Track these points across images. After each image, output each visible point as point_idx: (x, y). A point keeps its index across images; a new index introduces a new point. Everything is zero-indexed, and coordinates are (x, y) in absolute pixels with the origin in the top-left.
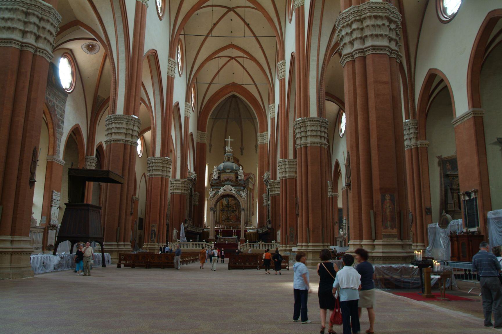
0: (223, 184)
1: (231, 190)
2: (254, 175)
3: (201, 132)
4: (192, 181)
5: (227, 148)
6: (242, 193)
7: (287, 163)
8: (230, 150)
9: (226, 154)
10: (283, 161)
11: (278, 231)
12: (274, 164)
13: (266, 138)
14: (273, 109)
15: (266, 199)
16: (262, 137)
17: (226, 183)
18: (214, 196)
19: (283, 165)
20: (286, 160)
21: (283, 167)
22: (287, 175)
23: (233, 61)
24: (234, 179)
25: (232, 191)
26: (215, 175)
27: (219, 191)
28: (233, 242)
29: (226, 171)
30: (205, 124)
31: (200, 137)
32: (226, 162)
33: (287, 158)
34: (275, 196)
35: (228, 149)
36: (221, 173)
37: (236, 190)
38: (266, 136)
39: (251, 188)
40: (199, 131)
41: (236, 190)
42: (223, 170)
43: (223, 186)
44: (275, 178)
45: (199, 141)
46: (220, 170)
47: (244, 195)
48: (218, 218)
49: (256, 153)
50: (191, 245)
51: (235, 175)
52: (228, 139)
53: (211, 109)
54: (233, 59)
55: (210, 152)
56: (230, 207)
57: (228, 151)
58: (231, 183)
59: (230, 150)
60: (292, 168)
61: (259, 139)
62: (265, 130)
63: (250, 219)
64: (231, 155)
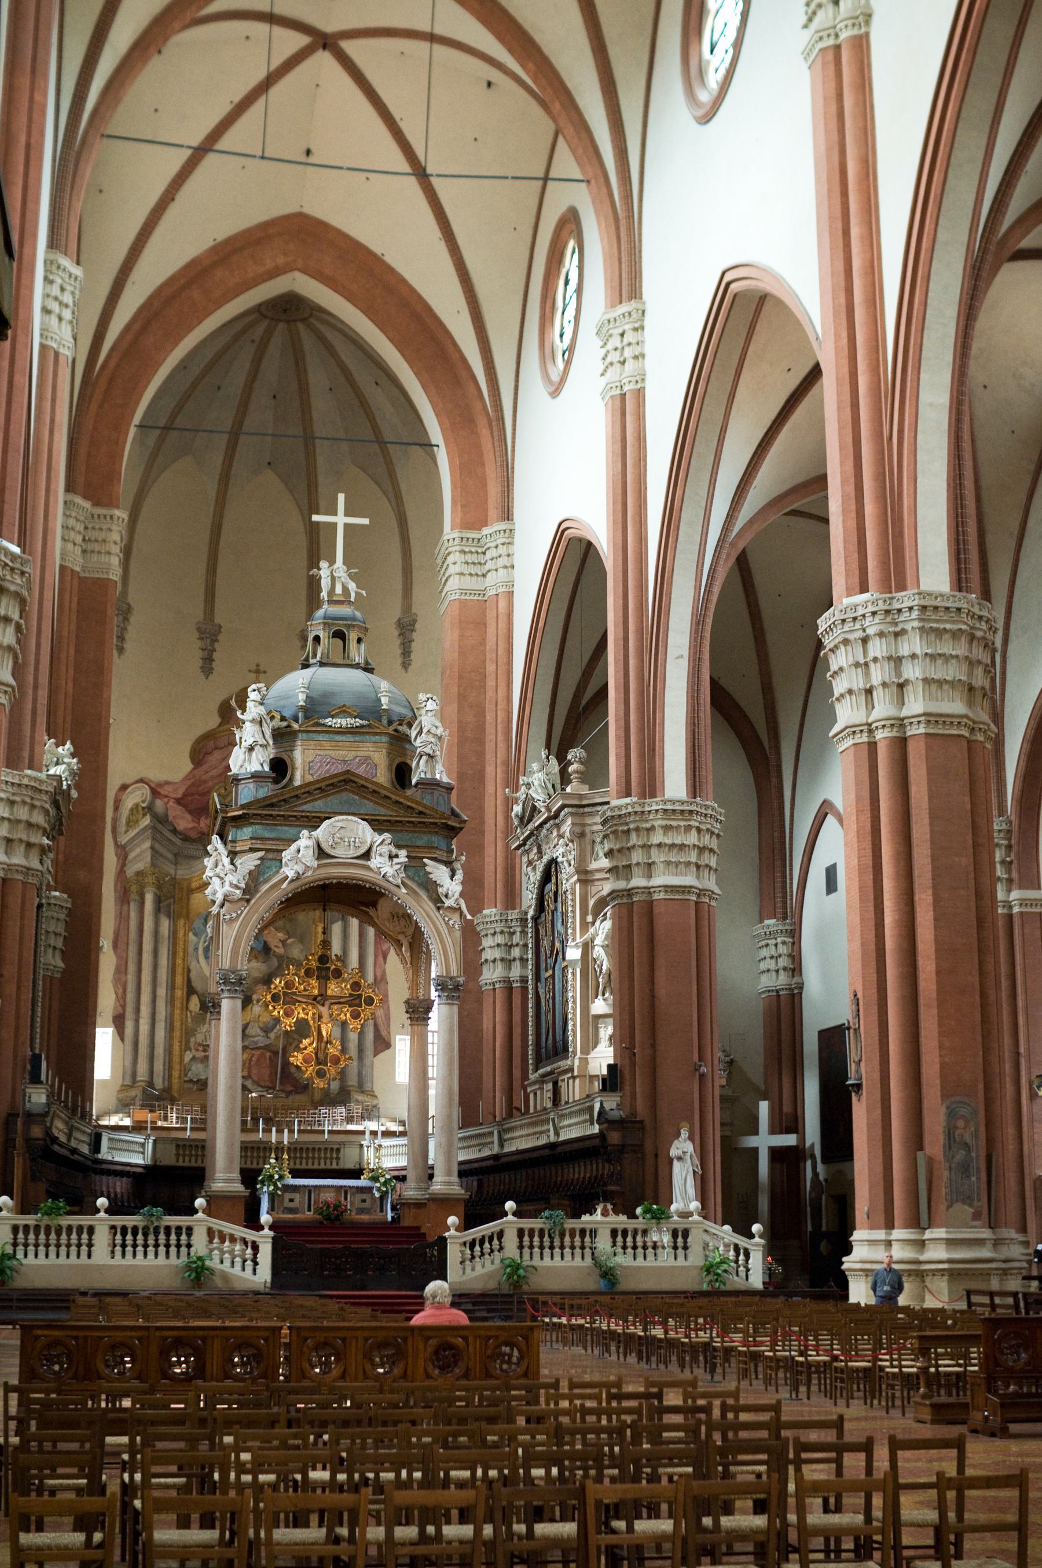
0: (319, 805)
1: (367, 855)
3: (87, 505)
4: (58, 797)
5: (324, 571)
6: (439, 873)
7: (911, 621)
8: (345, 589)
9: (320, 613)
10: (882, 606)
11: (679, 1135)
12: (641, 693)
13: (501, 562)
14: (629, 337)
15: (500, 939)
16: (469, 558)
17: (333, 801)
18: (250, 890)
19: (881, 634)
20: (906, 599)
21: (877, 648)
22: (915, 705)
23: (324, 60)
24: (383, 776)
25: (375, 862)
26: (251, 749)
27: (286, 855)
28: (365, 1217)
29: (329, 721)
30: (116, 456)
31: (79, 539)
32: (322, 664)
33: (902, 587)
34: (650, 904)
35: (333, 579)
36: (295, 733)
37: (403, 853)
38: (502, 550)
40: (78, 500)
41: (403, 853)
42: (306, 717)
43: (314, 822)
44: (651, 786)
45: (76, 564)
46: (287, 714)
47: (451, 886)
48: (159, 1066)
49: (406, 665)
50: (102, 1238)
51: (389, 754)
52: (335, 513)
53: (159, 364)
54: (325, 47)
55: (121, 650)
56: (338, 974)
57: (332, 591)
58: (369, 807)
59: (345, 589)
60: (946, 658)
61: (452, 569)
62: (493, 512)
63: (360, 1074)
64: (354, 619)
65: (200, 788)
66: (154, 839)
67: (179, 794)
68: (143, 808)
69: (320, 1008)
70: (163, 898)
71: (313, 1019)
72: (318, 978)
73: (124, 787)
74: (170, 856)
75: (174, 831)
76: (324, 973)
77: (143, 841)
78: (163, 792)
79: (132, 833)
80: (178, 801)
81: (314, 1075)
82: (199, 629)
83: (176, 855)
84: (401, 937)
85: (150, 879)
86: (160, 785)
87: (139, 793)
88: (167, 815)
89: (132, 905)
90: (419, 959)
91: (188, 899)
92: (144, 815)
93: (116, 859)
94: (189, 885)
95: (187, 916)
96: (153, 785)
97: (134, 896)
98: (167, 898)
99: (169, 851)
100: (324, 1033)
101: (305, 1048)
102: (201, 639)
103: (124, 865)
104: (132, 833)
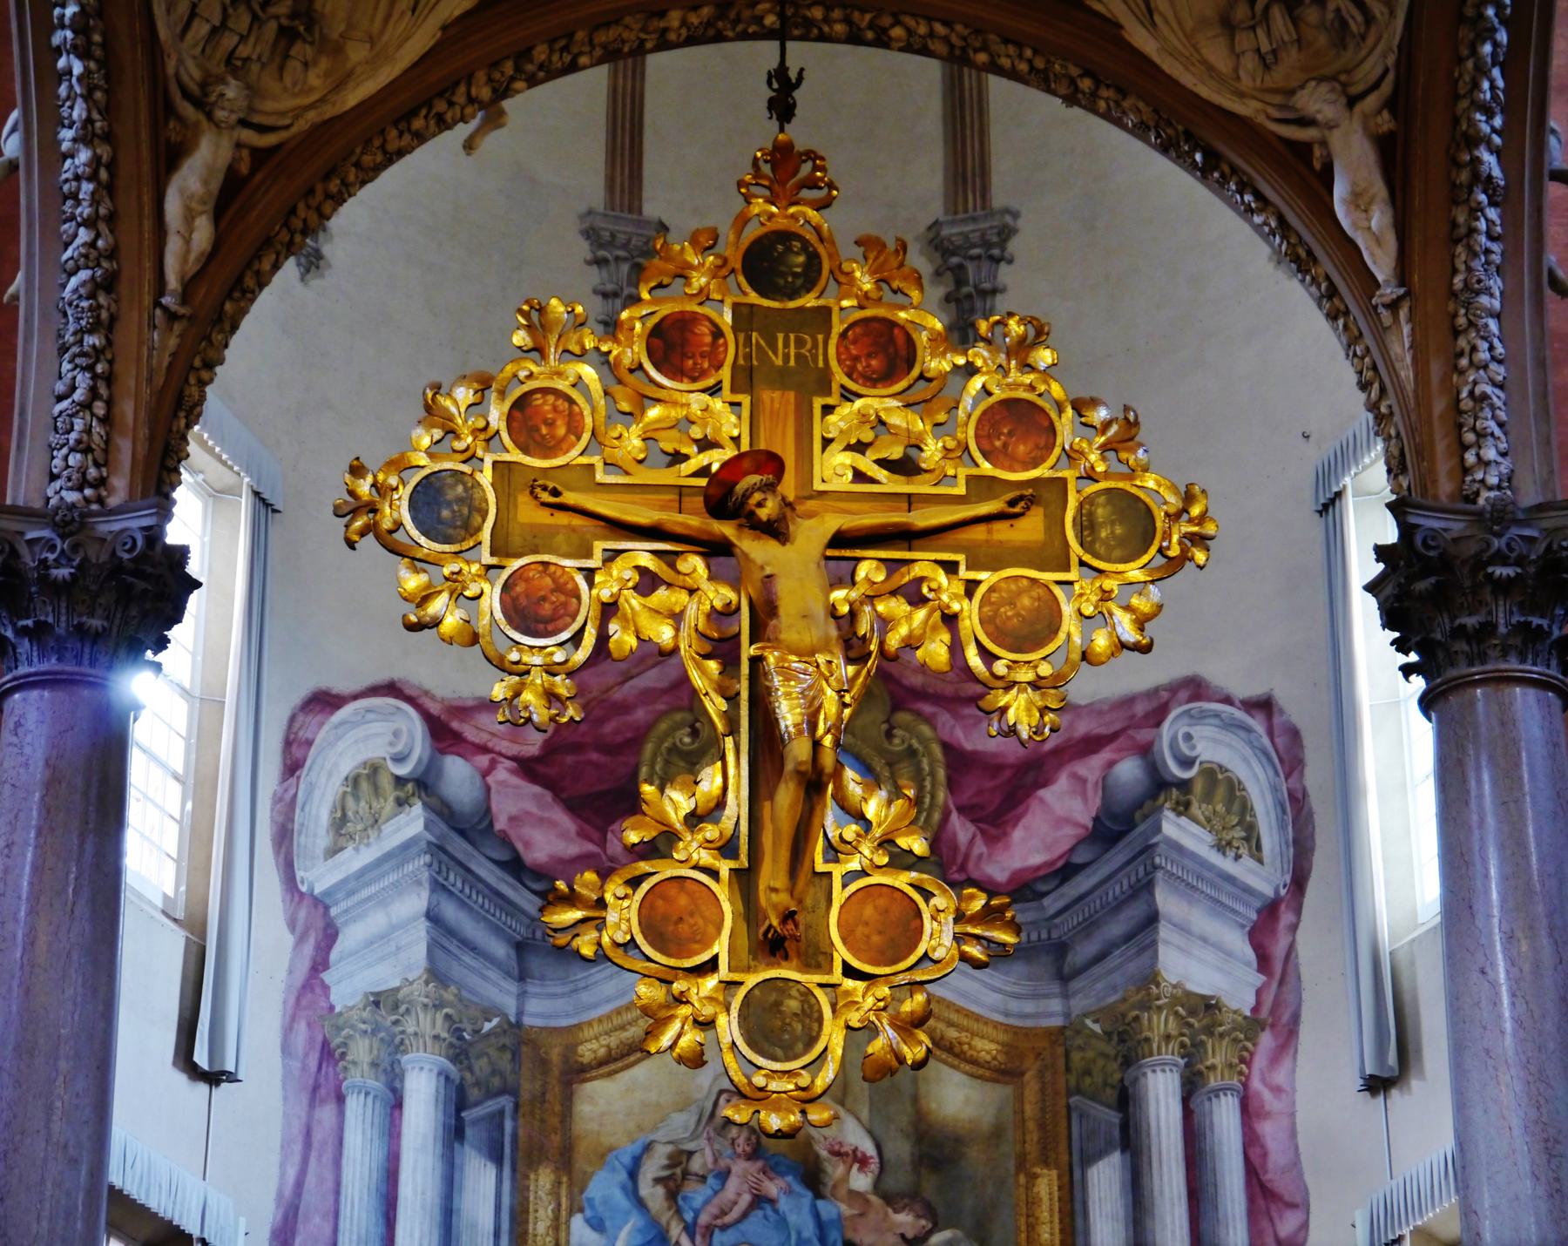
2: (1264, 706)
39: (1209, 1006)
65: (608, 728)
66: (438, 887)
67: (533, 744)
68: (399, 781)
69: (757, 550)
70: (474, 1094)
71: (723, 649)
72: (745, 379)
73: (324, 702)
74: (500, 950)
75: (515, 866)
76: (783, 352)
77: (398, 889)
78: (470, 733)
79: (354, 859)
80: (527, 768)
81: (728, 1027)
82: (590, 234)
83: (520, 947)
84: (1318, 102)
85: (425, 1024)
86: (463, 711)
87: (377, 727)
88: (487, 812)
89: (354, 1104)
90: (1460, 236)
91: (568, 1099)
92: (401, 803)
93: (289, 940)
94: (571, 1048)
95: (565, 1159)
96: (435, 709)
97: (360, 1076)
98: (491, 1094)
99: (497, 931)
100: (788, 714)
101: (661, 845)
102: (599, 262)
103: (320, 964)
104: (354, 859)
